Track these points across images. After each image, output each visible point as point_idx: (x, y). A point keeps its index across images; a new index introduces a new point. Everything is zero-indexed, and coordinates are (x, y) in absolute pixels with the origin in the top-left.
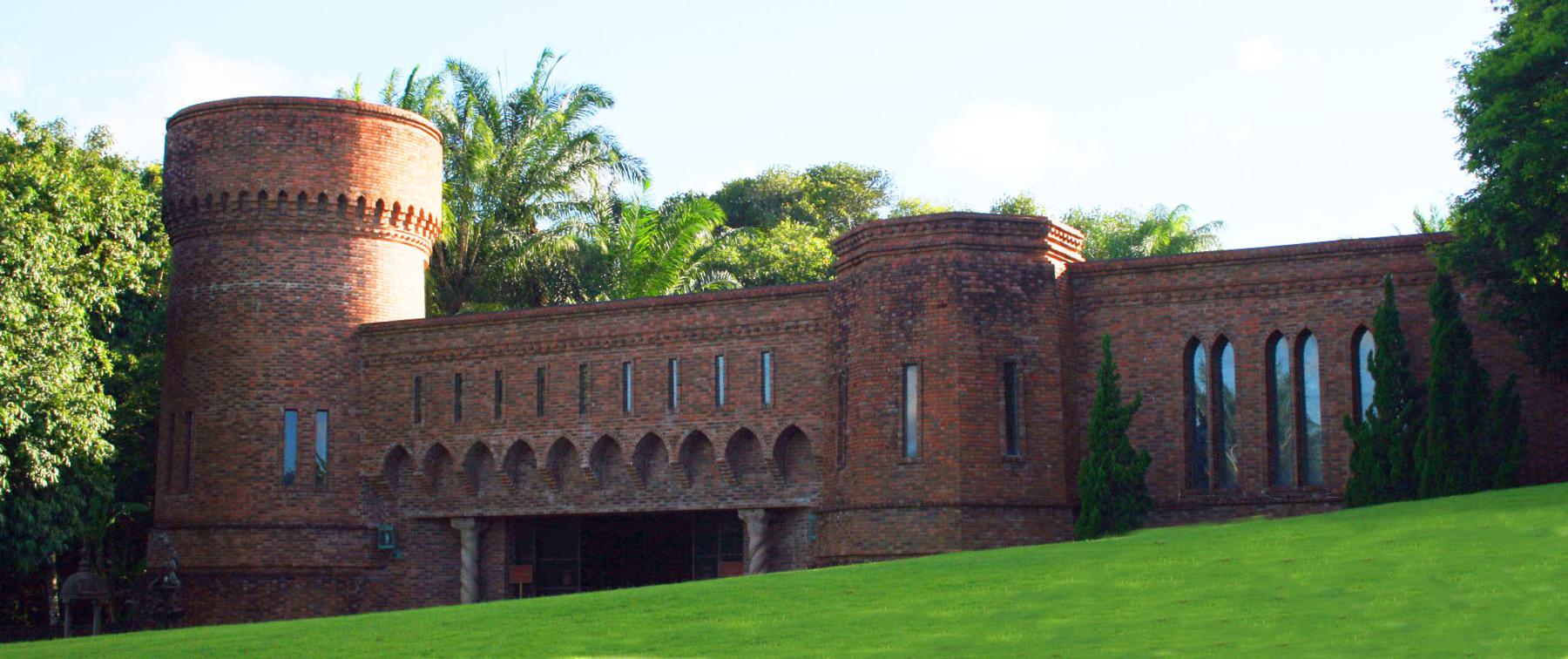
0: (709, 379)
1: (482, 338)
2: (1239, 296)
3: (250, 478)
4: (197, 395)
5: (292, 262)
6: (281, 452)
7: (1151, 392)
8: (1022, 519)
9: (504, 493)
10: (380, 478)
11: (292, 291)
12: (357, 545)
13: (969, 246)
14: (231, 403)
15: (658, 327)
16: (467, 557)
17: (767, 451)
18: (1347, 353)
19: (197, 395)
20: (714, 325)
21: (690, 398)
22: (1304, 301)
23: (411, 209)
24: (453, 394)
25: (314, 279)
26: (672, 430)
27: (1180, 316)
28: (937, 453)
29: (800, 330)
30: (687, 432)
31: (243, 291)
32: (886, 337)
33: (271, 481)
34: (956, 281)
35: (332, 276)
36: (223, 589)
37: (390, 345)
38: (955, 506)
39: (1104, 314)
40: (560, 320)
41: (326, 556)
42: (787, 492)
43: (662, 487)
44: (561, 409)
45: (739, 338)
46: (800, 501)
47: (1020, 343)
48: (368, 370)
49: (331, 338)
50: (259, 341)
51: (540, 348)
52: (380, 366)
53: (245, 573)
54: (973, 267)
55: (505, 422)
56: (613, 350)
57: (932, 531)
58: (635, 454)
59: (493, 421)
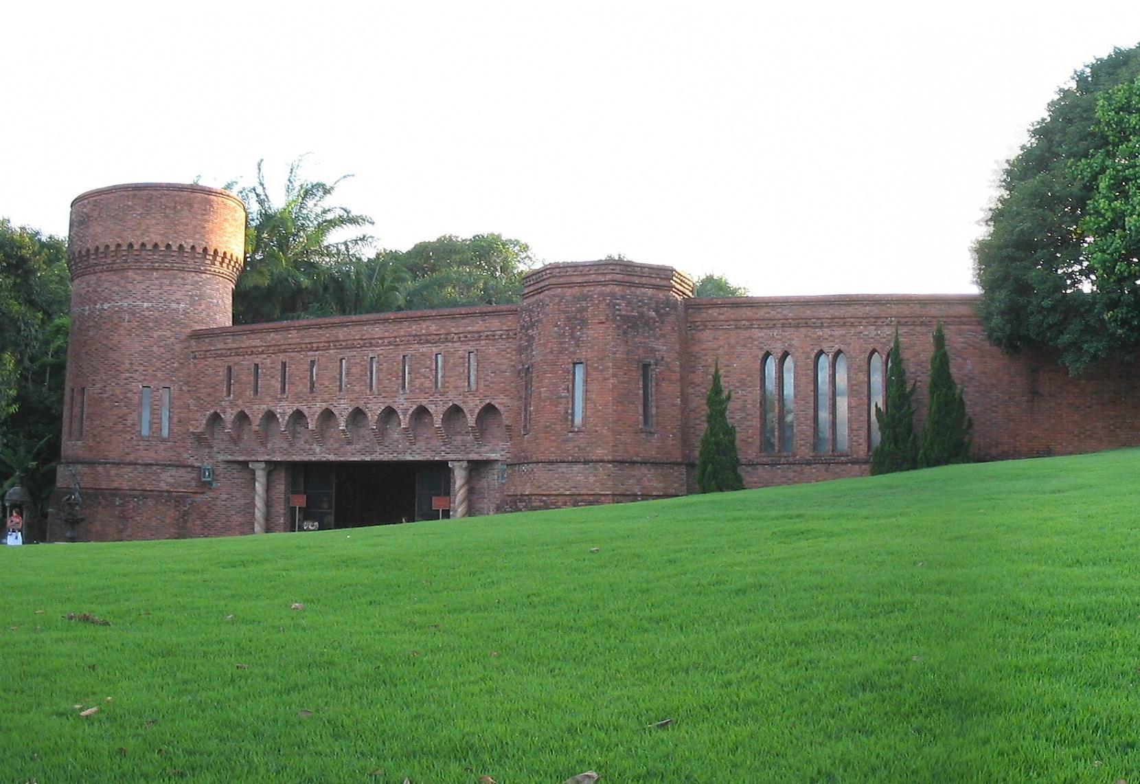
0: (431, 370)
1: (273, 339)
2: (797, 326)
3: (121, 431)
4: (88, 377)
5: (148, 289)
6: (140, 415)
7: (738, 387)
8: (652, 471)
9: (285, 445)
10: (203, 433)
11: (147, 308)
12: (188, 477)
13: (620, 283)
14: (109, 382)
15: (395, 334)
16: (259, 487)
17: (471, 421)
18: (865, 367)
19: (88, 377)
20: (435, 332)
21: (417, 383)
22: (838, 332)
23: (225, 253)
24: (252, 378)
25: (161, 300)
26: (404, 405)
27: (759, 337)
28: (596, 426)
29: (496, 337)
30: (415, 407)
31: (117, 309)
32: (562, 343)
34: (612, 306)
35: (174, 299)
36: (104, 503)
37: (211, 344)
38: (609, 462)
39: (707, 335)
40: (327, 328)
41: (167, 484)
42: (483, 449)
43: (396, 443)
44: (326, 389)
45: (453, 342)
46: (493, 456)
47: (653, 350)
48: (196, 361)
49: (172, 339)
50: (126, 341)
51: (312, 347)
53: (115, 492)
54: (623, 297)
55: (287, 397)
56: (364, 349)
57: (592, 479)
58: (378, 420)
59: (279, 396)
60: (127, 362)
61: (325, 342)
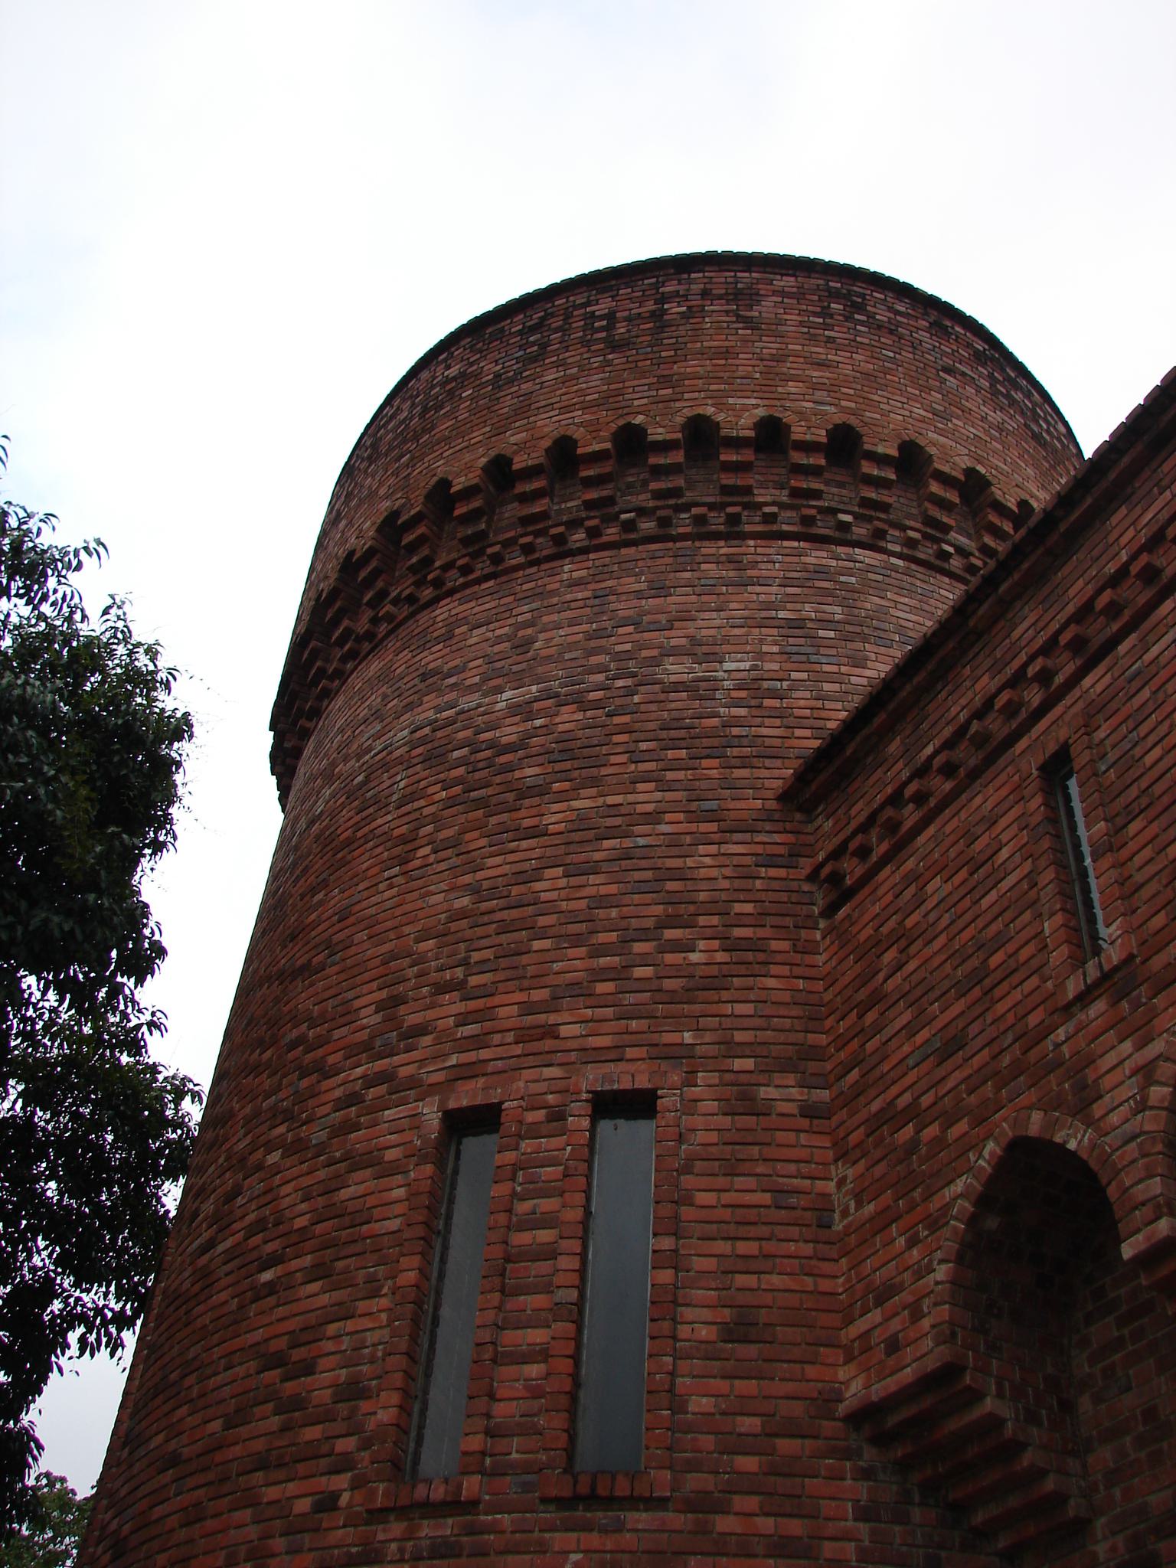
3: (262, 1463)
11: (514, 709)
33: (344, 1464)
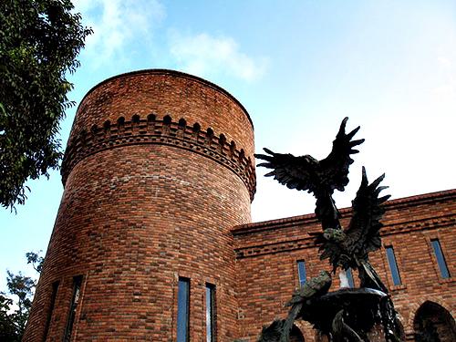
11: (185, 186)
40: (442, 202)
52: (254, 256)
60: (156, 243)
61: (444, 216)
